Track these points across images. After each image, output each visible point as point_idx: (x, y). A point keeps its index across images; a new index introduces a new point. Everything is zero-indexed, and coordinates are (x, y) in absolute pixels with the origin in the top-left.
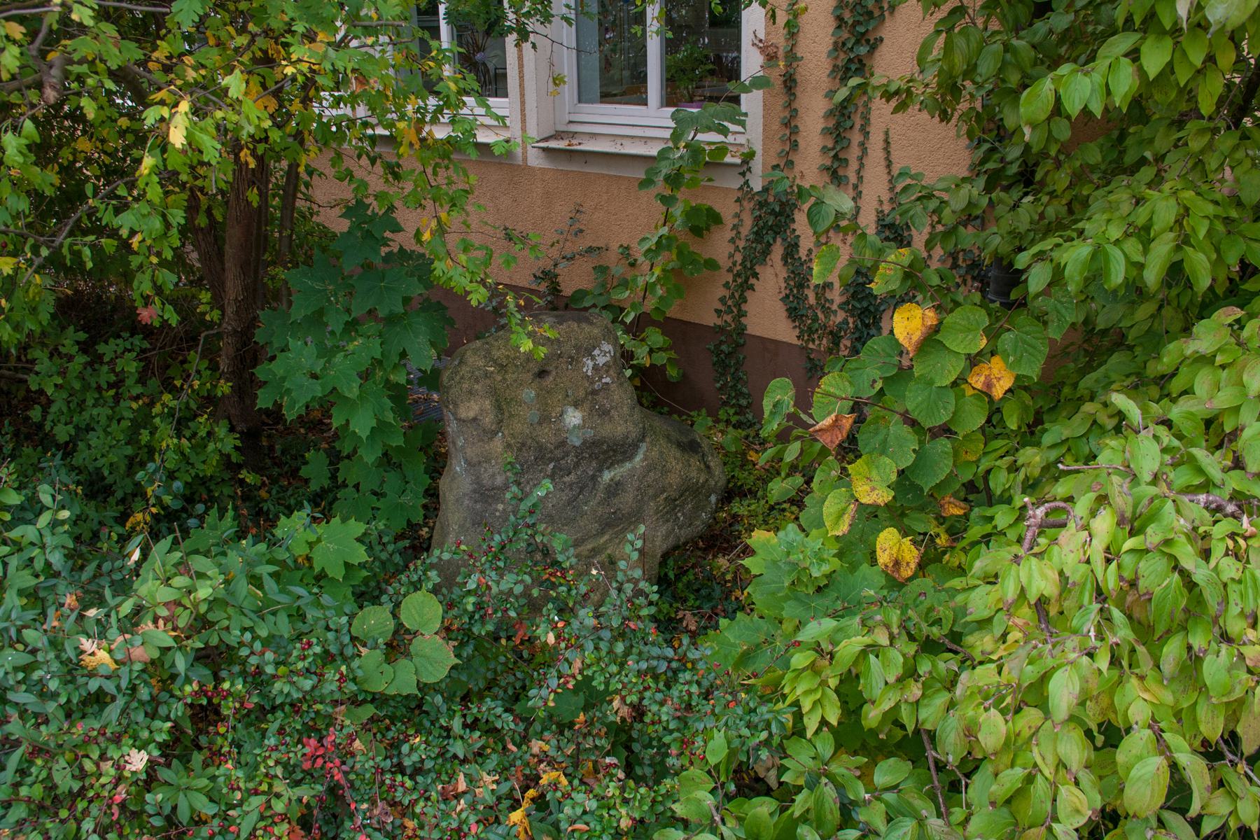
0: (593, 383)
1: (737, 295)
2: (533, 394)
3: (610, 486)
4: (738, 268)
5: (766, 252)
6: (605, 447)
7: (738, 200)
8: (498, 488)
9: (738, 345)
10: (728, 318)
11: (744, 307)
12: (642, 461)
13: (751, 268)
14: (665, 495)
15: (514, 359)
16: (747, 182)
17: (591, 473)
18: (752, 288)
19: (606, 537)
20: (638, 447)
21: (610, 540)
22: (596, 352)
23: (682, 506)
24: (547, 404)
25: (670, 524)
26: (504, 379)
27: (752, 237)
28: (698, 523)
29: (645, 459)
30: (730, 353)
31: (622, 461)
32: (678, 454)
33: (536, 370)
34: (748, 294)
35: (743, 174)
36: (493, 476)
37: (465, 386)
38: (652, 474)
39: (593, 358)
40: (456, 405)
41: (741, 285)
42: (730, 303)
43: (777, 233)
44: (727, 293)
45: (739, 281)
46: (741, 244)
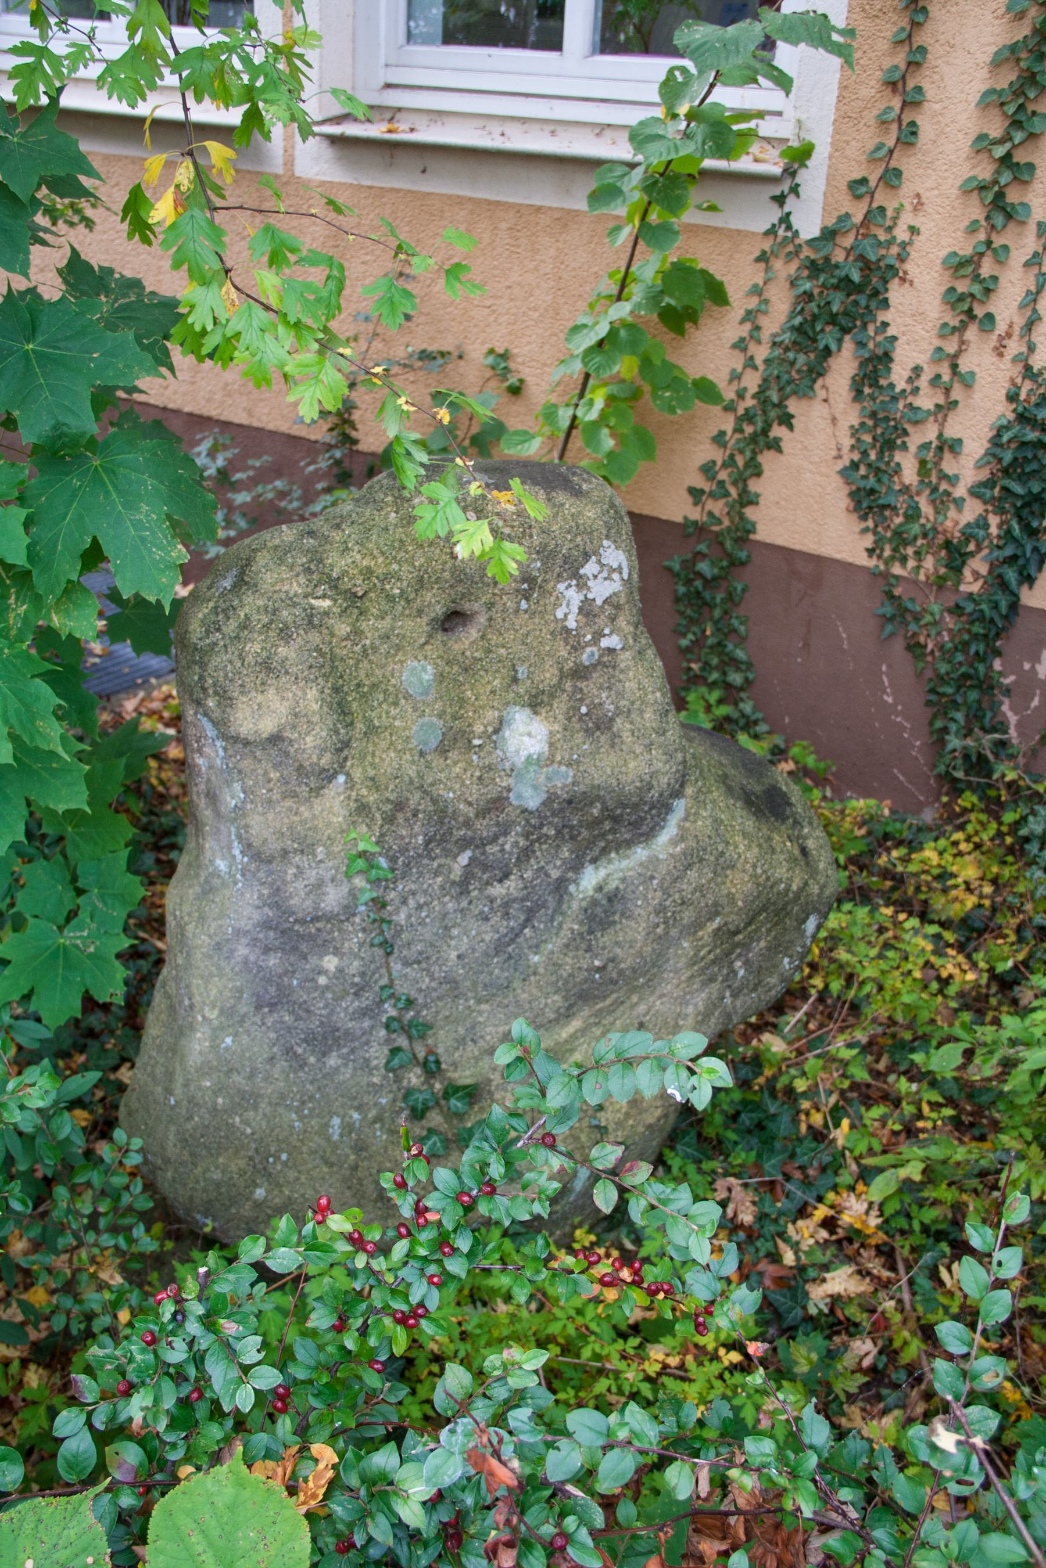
0: (578, 648)
1: (740, 461)
2: (428, 674)
3: (594, 903)
4: (749, 402)
5: (816, 372)
6: (595, 812)
7: (763, 258)
8: (328, 918)
10: (717, 507)
11: (754, 486)
12: (674, 842)
13: (780, 405)
14: (717, 921)
15: (386, 578)
16: (786, 219)
17: (555, 874)
18: (775, 445)
19: (576, 1024)
20: (668, 809)
21: (583, 1031)
22: (590, 569)
23: (745, 946)
24: (462, 701)
25: (715, 987)
26: (357, 632)
27: (787, 337)
28: (773, 980)
29: (682, 838)
30: (715, 579)
31: (629, 844)
32: (750, 824)
33: (439, 610)
34: (766, 459)
35: (780, 200)
36: (318, 886)
37: (254, 647)
38: (692, 874)
39: (582, 584)
40: (226, 699)
41: (753, 439)
42: (723, 475)
43: (845, 331)
44: (718, 456)
45: (749, 430)
46: (761, 353)
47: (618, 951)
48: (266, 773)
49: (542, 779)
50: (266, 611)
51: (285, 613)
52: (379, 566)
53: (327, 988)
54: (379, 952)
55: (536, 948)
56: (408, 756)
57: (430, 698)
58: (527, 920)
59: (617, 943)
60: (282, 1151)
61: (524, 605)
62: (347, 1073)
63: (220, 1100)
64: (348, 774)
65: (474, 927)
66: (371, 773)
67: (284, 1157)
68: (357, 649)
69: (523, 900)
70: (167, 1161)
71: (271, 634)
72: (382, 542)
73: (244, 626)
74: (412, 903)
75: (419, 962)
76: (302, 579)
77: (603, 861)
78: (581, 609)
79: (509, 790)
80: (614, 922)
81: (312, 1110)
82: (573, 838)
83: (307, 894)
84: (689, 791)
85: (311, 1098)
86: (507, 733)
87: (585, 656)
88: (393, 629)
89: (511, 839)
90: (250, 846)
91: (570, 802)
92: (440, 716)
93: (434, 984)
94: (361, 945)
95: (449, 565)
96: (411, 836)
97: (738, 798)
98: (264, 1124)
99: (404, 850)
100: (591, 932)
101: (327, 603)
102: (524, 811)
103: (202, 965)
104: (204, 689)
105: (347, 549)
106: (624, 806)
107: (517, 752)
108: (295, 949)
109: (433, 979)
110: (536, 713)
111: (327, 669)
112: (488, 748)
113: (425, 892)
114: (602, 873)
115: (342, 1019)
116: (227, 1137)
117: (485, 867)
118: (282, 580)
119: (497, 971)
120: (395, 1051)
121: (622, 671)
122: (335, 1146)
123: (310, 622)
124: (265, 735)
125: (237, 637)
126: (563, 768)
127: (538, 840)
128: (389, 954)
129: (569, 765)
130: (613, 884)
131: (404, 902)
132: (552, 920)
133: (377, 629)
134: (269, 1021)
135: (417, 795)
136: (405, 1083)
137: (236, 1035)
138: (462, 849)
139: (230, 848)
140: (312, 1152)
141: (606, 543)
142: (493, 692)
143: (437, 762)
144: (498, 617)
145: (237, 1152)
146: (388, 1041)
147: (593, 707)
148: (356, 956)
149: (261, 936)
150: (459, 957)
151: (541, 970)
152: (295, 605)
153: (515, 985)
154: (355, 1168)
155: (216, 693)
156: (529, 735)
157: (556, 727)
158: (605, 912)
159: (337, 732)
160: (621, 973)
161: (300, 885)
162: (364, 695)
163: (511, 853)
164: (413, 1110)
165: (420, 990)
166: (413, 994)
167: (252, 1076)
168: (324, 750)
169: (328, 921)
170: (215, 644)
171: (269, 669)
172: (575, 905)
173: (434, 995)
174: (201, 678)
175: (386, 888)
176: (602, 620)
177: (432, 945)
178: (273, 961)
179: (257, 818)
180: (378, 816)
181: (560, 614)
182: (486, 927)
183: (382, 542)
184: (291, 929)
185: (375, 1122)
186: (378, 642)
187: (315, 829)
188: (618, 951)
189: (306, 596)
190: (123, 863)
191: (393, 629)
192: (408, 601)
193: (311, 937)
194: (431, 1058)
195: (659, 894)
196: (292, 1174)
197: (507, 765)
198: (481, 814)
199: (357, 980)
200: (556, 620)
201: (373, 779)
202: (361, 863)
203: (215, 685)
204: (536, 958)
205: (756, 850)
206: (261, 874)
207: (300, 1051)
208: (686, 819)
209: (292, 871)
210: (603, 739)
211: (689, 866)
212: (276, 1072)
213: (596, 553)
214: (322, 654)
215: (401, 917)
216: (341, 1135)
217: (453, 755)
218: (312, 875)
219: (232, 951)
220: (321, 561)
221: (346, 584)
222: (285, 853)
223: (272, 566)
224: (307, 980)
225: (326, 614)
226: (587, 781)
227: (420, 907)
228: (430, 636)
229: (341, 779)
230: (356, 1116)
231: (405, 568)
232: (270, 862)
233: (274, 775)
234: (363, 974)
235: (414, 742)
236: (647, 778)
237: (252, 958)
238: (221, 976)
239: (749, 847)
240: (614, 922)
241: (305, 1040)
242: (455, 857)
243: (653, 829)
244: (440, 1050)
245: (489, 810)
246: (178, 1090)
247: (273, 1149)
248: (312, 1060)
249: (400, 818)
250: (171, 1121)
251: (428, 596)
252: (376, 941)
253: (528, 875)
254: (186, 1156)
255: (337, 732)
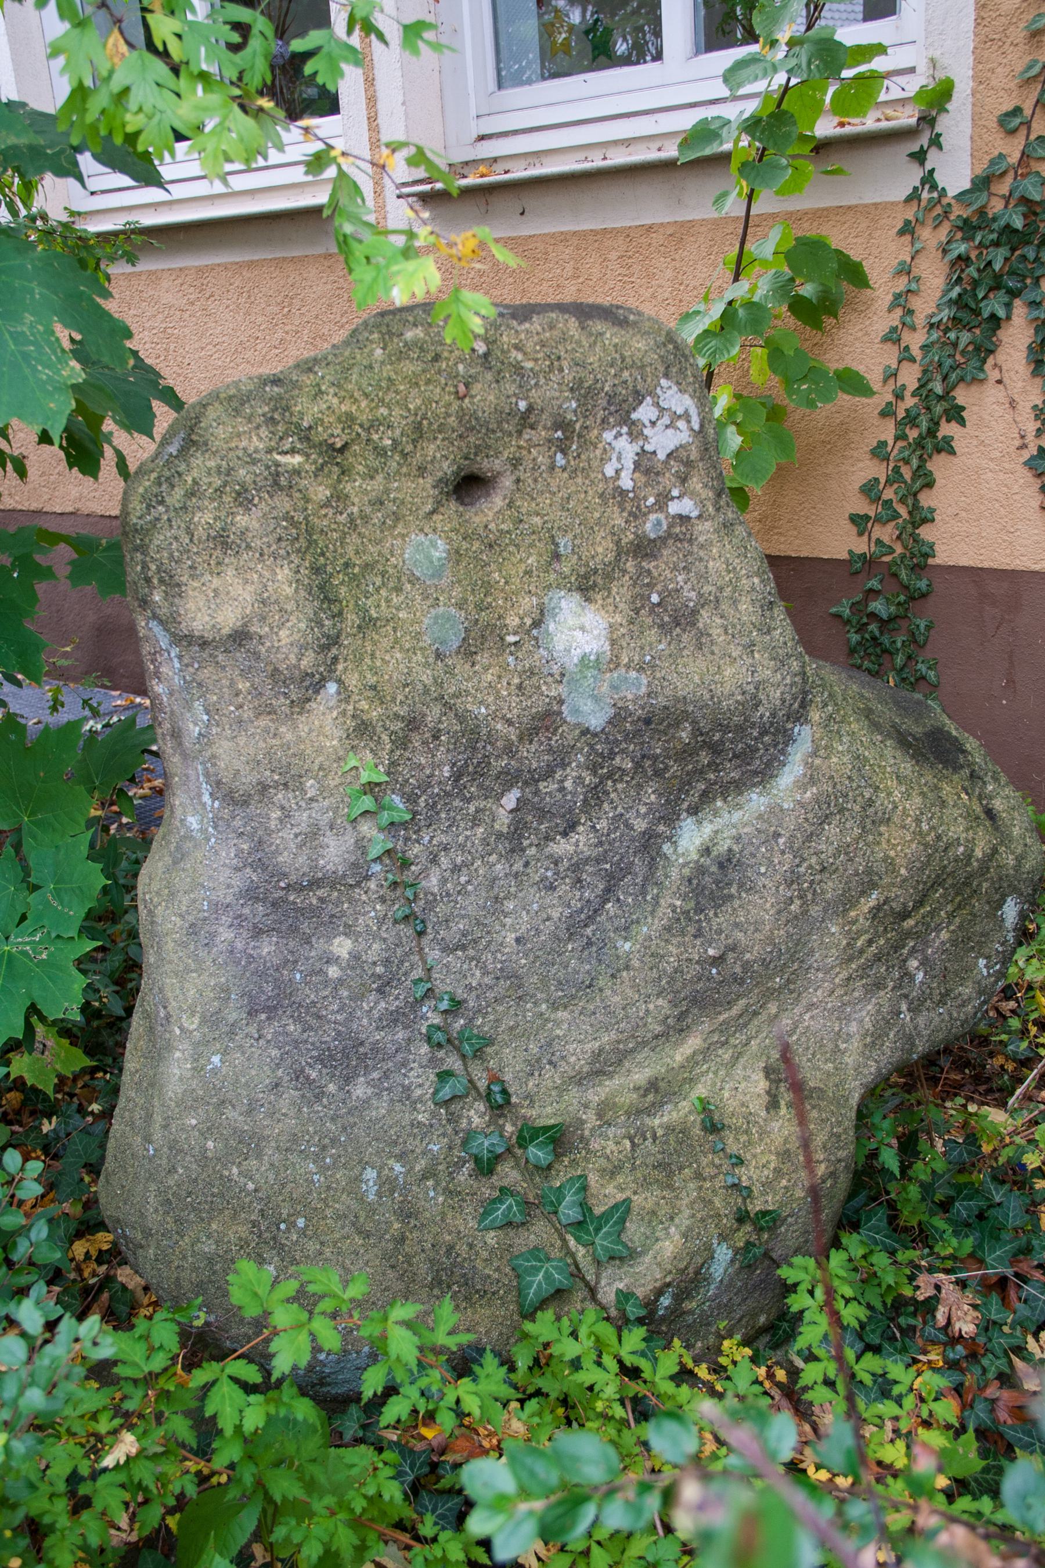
0: (637, 515)
1: (907, 473)
2: (439, 550)
3: (701, 870)
4: (910, 402)
5: (984, 351)
6: (684, 735)
7: (907, 229)
8: (333, 882)
9: (919, 597)
10: (886, 533)
11: (926, 500)
12: (802, 785)
13: (946, 396)
14: (874, 899)
15: (372, 425)
16: (929, 180)
17: (640, 825)
18: (946, 447)
19: (693, 1043)
20: (789, 739)
21: (706, 1052)
22: (645, 412)
23: (920, 935)
24: (488, 587)
25: (884, 996)
26: (339, 498)
27: (945, 314)
28: (966, 990)
29: (811, 779)
30: (892, 619)
31: (739, 786)
32: (907, 767)
33: (447, 468)
34: (938, 465)
35: (919, 157)
36: (312, 836)
37: (205, 517)
38: (831, 830)
39: (636, 432)
40: (173, 587)
41: (919, 444)
42: (889, 494)
43: (1014, 294)
44: (880, 471)
45: (913, 434)
46: (915, 340)
47: (740, 935)
48: (232, 683)
49: (605, 688)
50: (219, 472)
51: (242, 472)
52: (362, 409)
53: (341, 981)
54: (406, 931)
55: (626, 930)
56: (419, 657)
57: (444, 582)
58: (608, 890)
59: (736, 925)
60: (298, 1214)
61: (559, 458)
62: (381, 1108)
63: (210, 1144)
64: (339, 681)
65: (535, 898)
66: (372, 680)
67: (301, 1222)
68: (342, 518)
69: (598, 861)
70: (148, 1234)
71: (227, 499)
72: (364, 382)
73: (191, 494)
74: (444, 861)
75: (464, 948)
76: (264, 432)
77: (706, 812)
78: (637, 466)
79: (561, 702)
80: (731, 897)
81: (336, 1158)
82: (658, 774)
83: (300, 847)
84: (815, 715)
85: (334, 1141)
86: (552, 627)
87: (648, 526)
88: (387, 491)
89: (572, 772)
90: (219, 783)
91: (648, 722)
92: (460, 606)
93: (487, 980)
94: (381, 921)
95: (455, 406)
96: (434, 766)
97: (889, 736)
98: (271, 1176)
99: (425, 785)
100: (700, 910)
101: (297, 459)
102: (586, 732)
103: (174, 957)
104: (148, 580)
105: (321, 392)
106: (725, 729)
107: (568, 651)
108: (294, 930)
109: (486, 973)
110: (588, 600)
111: (303, 543)
112: (527, 646)
113: (462, 847)
114: (708, 829)
115: (365, 1026)
116: (222, 1195)
117: (543, 814)
118: (239, 435)
119: (579, 967)
120: (444, 1076)
121: (702, 547)
122: (372, 1210)
123: (276, 483)
124: (226, 631)
125: (184, 508)
126: (633, 674)
127: (610, 776)
128: (421, 934)
129: (641, 669)
130: (723, 846)
131: (434, 860)
132: (644, 893)
133: (366, 492)
134: (269, 1033)
135: (436, 710)
136: (464, 1124)
137: (225, 1052)
138: (507, 788)
139: (200, 795)
140: (339, 1217)
141: (664, 382)
142: (528, 573)
143: (462, 668)
144: (526, 476)
145: (234, 1216)
146: (433, 1061)
147: (667, 595)
148: (375, 937)
149: (246, 911)
150: (518, 940)
151: (636, 963)
152: (254, 462)
153: (601, 983)
154: (402, 1240)
155: (162, 581)
156: (582, 629)
157: (618, 618)
158: (717, 882)
159: (320, 624)
160: (746, 966)
161: (288, 834)
162: (354, 577)
163: (574, 794)
164: (477, 1160)
165: (470, 988)
166: (460, 994)
167: (250, 1112)
168: (304, 647)
169: (333, 888)
170: (158, 519)
171: (226, 545)
172: (674, 873)
173: (490, 995)
174: (145, 567)
175: (407, 839)
176: (667, 480)
177: (478, 923)
178: (267, 948)
179: (226, 744)
180: (385, 738)
181: (609, 471)
182: (551, 899)
183: (364, 382)
184: (284, 900)
185: (425, 1177)
186: (368, 510)
187: (301, 755)
188: (740, 935)
189: (269, 451)
190: (84, 849)
191: (387, 491)
192: (404, 455)
193: (313, 912)
194: (496, 1088)
195: (788, 856)
196: (312, 1247)
197: (555, 669)
198: (528, 734)
199: (380, 970)
200: (606, 479)
201: (374, 688)
202: (367, 802)
203: (159, 570)
204: (627, 946)
205: (918, 800)
206: (237, 823)
207: (314, 1075)
208: (815, 754)
209: (276, 814)
210: (685, 637)
211: (826, 819)
212: (284, 1105)
213: (651, 393)
214: (294, 524)
215: (432, 882)
216: (379, 1194)
217: (483, 659)
218: (303, 818)
219: (213, 935)
220: (287, 409)
221: (321, 434)
222: (263, 788)
223: (224, 418)
224: (313, 973)
225: (297, 472)
226: (668, 692)
227: (456, 869)
228: (439, 503)
229: (332, 688)
230: (398, 1168)
231: (397, 412)
232: (246, 803)
233: (243, 685)
234: (387, 962)
235: (427, 640)
236: (751, 688)
237: (239, 945)
238: (199, 971)
239: (907, 795)
240: (731, 897)
241: (319, 1059)
242: (499, 797)
243: (768, 764)
244: (508, 1077)
245: (536, 730)
246: (157, 1136)
247: (285, 1212)
248: (332, 1088)
249: (416, 741)
250: (151, 1177)
251: (431, 449)
252: (400, 914)
253: (602, 825)
254: (171, 1225)
255: (320, 624)
